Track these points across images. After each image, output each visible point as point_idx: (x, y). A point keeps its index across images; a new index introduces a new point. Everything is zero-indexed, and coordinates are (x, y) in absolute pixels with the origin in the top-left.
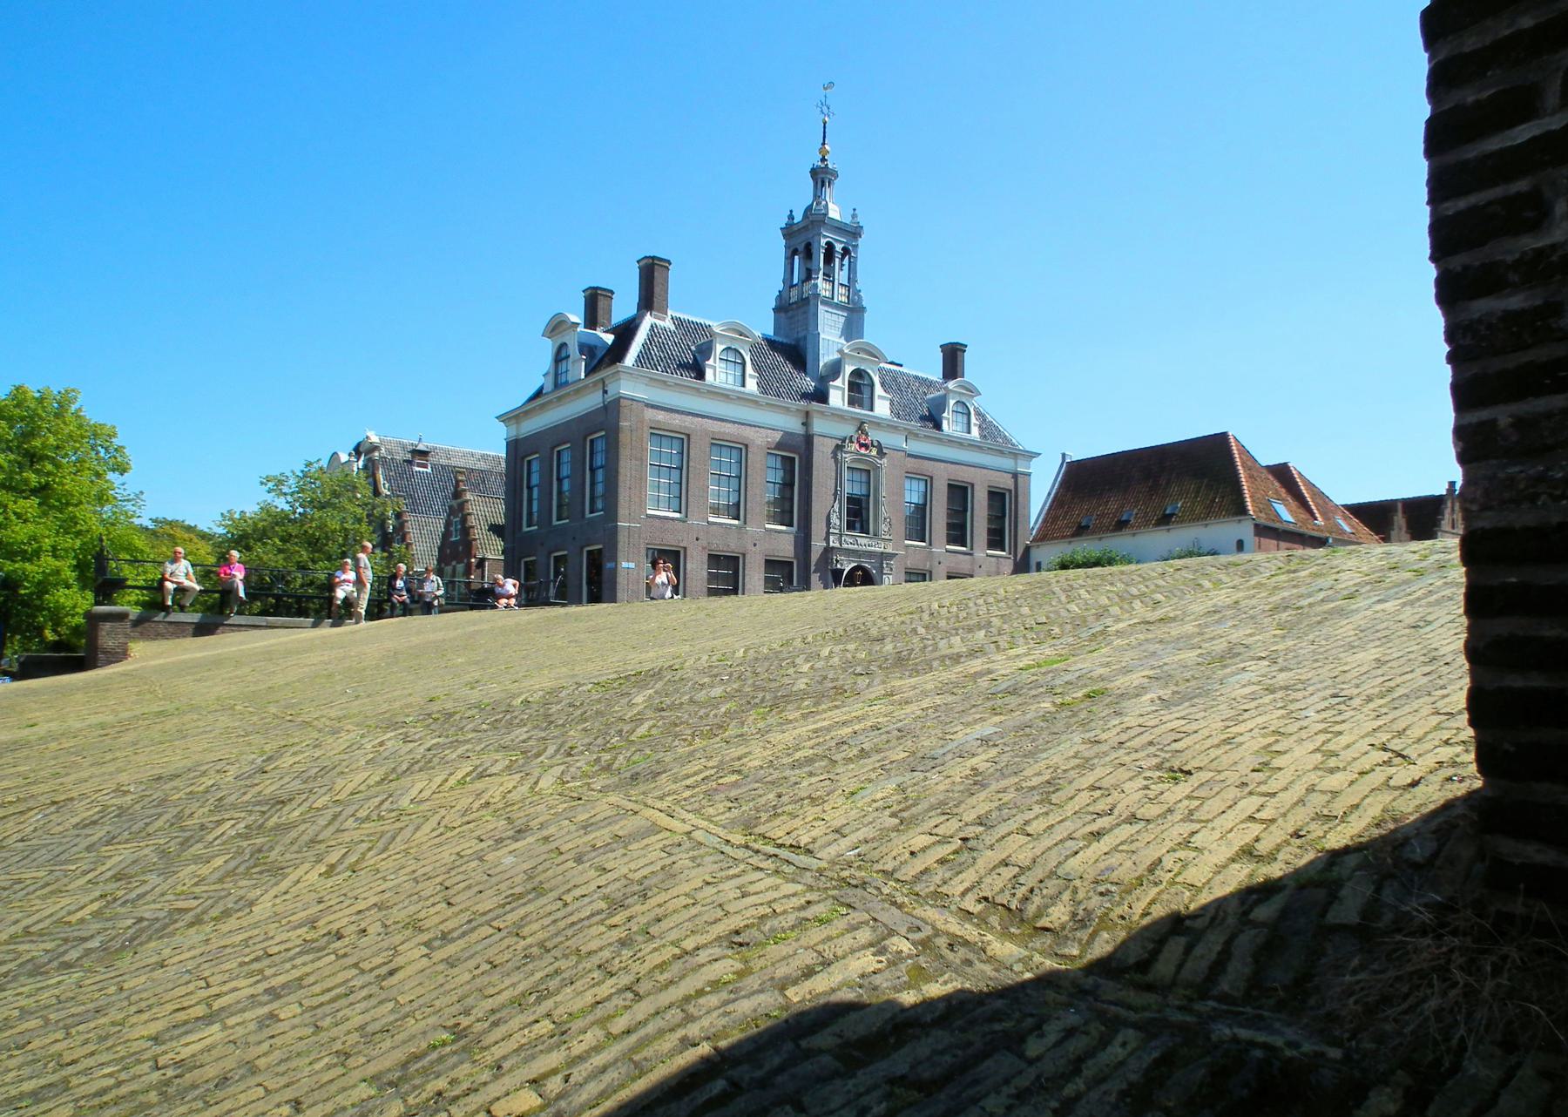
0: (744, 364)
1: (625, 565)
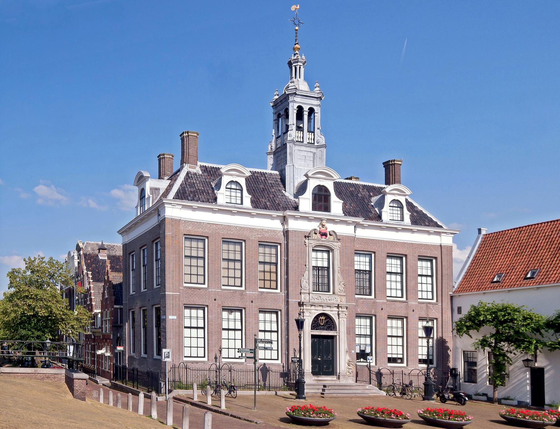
0: (242, 190)
1: (171, 317)
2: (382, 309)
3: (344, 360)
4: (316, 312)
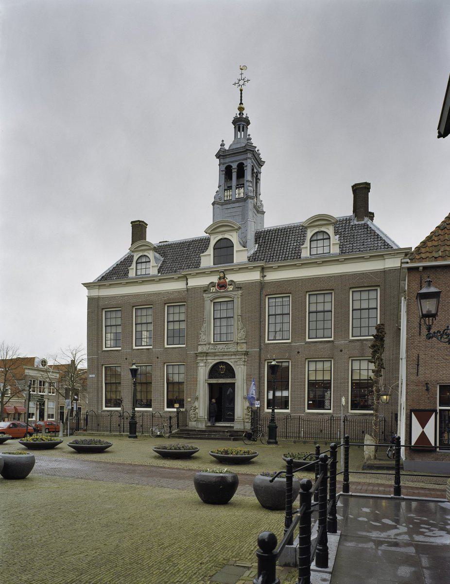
2: (298, 352)
3: (240, 408)
4: (212, 361)
